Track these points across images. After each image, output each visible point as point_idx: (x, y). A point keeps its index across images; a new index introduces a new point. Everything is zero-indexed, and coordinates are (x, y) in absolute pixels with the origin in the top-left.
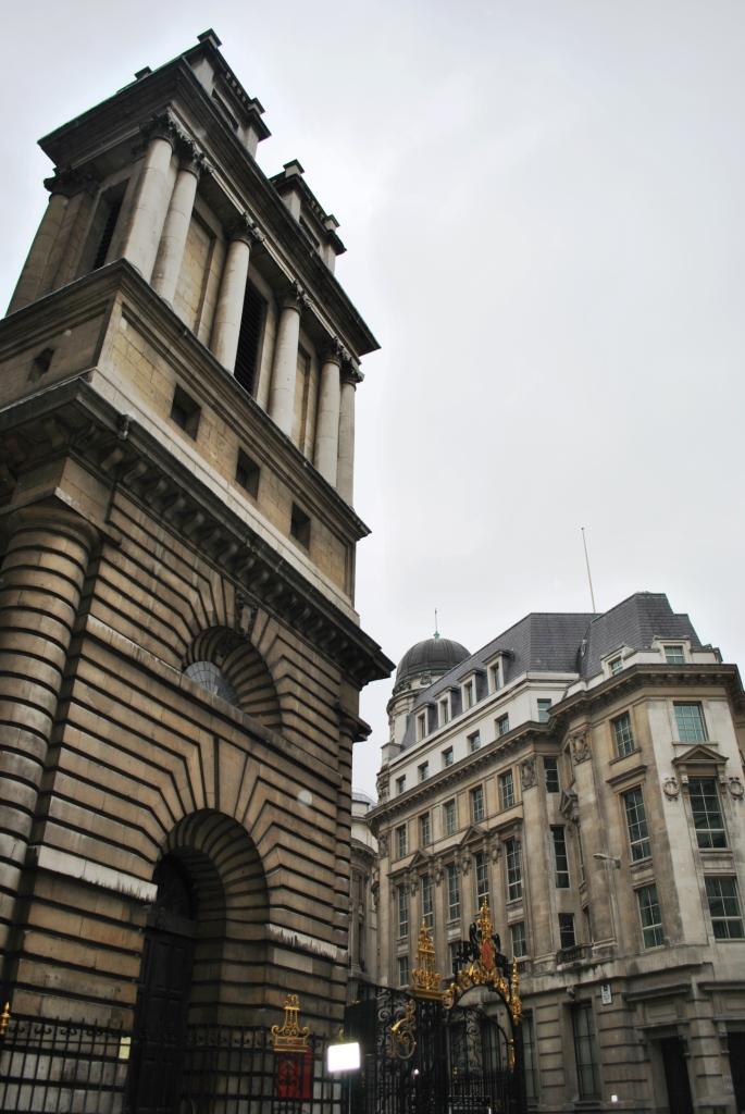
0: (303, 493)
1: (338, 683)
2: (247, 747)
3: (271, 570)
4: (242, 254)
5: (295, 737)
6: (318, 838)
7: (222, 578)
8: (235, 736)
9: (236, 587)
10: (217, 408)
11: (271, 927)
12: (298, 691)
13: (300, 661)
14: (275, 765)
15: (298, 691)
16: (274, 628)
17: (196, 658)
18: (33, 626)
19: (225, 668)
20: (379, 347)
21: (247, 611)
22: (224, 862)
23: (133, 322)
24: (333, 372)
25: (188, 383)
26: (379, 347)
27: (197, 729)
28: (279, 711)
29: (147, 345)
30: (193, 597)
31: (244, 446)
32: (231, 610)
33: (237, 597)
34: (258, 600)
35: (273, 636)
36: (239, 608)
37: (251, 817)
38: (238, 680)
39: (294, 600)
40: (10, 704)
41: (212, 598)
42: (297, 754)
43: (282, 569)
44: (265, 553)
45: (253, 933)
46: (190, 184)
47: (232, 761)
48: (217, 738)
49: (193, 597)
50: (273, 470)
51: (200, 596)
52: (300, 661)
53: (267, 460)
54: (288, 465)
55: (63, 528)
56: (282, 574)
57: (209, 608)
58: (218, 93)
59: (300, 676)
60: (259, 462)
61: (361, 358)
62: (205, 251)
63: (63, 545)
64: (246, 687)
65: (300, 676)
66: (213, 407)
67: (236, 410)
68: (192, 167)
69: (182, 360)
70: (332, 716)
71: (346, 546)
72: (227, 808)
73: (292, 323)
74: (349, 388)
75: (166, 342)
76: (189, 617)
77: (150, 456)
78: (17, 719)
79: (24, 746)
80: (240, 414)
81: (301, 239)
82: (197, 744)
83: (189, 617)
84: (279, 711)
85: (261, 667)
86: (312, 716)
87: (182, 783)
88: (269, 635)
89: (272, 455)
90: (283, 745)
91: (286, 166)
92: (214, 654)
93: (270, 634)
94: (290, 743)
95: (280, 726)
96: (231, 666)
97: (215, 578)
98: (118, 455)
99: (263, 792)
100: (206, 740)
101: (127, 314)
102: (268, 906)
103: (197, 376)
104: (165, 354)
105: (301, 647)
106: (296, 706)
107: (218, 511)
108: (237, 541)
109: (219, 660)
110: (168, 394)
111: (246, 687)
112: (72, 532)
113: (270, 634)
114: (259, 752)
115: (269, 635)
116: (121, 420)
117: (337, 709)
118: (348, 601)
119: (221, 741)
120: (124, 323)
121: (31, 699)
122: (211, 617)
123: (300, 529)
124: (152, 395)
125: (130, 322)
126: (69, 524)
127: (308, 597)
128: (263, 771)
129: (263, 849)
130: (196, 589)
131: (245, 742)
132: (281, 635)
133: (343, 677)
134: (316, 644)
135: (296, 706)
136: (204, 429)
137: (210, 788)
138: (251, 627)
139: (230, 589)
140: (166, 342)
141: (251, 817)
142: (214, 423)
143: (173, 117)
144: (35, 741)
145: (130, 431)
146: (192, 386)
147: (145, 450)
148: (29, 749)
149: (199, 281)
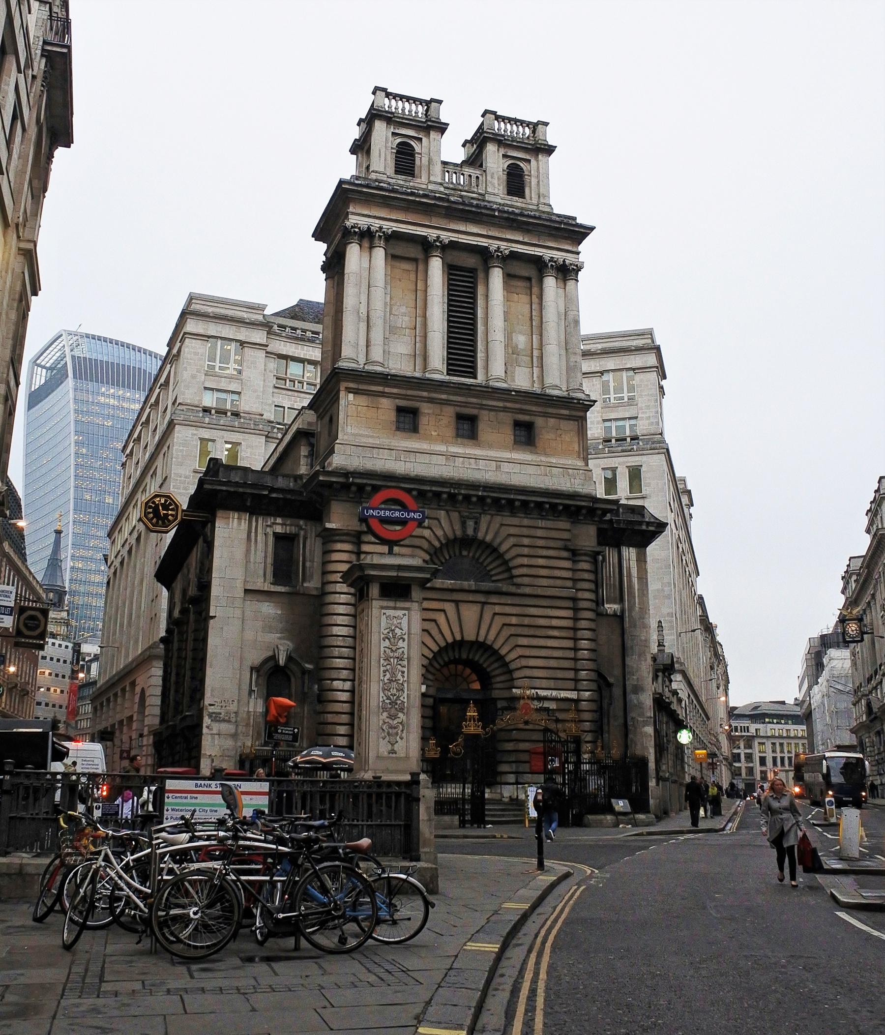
0: (521, 409)
1: (569, 530)
2: (483, 600)
3: (477, 496)
4: (436, 265)
5: (526, 580)
6: (556, 633)
7: (447, 511)
8: (471, 597)
9: (459, 512)
10: (431, 401)
11: (514, 690)
12: (526, 551)
13: (525, 531)
14: (509, 602)
15: (526, 551)
16: (498, 520)
17: (447, 558)
18: (333, 590)
19: (471, 555)
20: (592, 229)
21: (471, 524)
22: (485, 661)
23: (356, 392)
24: (550, 282)
25: (404, 399)
26: (592, 229)
27: (442, 603)
28: (509, 569)
29: (370, 398)
30: (427, 533)
31: (458, 409)
32: (457, 527)
33: (461, 517)
34: (480, 511)
35: (498, 525)
36: (464, 524)
37: (491, 637)
38: (481, 560)
39: (503, 502)
40: (330, 628)
41: (443, 525)
42: (527, 590)
43: (484, 491)
44: (466, 489)
45: (506, 694)
46: (379, 254)
47: (470, 613)
48: (457, 602)
49: (427, 533)
50: (490, 410)
51: (432, 530)
52: (525, 531)
53: (482, 407)
54: (499, 400)
55: (337, 538)
56: (485, 494)
57: (440, 533)
58: (397, 131)
59: (526, 541)
60: (474, 412)
61: (581, 248)
62: (412, 276)
63: (339, 546)
64: (489, 560)
65: (526, 541)
66: (428, 402)
67: (443, 393)
68: (376, 242)
69: (395, 391)
70: (565, 554)
71: (577, 420)
72: (470, 636)
73: (497, 276)
74: (570, 284)
75: (380, 389)
76: (426, 545)
77: (369, 482)
78: (334, 633)
79: (339, 644)
80: (449, 394)
81: (483, 211)
82: (444, 611)
83: (426, 545)
84: (509, 569)
85: (492, 549)
86: (541, 562)
87: (435, 632)
88: (490, 528)
89: (484, 402)
90: (513, 589)
91: (483, 116)
92: (460, 553)
93: (495, 526)
94: (518, 585)
95: (512, 577)
96: (476, 552)
97: (443, 513)
98: (354, 488)
99: (499, 621)
100: (449, 607)
101: (349, 390)
102: (513, 680)
103: (410, 392)
104: (383, 395)
105: (526, 522)
106: (525, 561)
107: (424, 484)
108: (445, 492)
109: (465, 553)
110: (392, 416)
111: (489, 560)
112: (344, 538)
113: (495, 526)
114: (494, 599)
115: (490, 528)
116: (347, 474)
117: (566, 549)
118: (580, 463)
119: (461, 604)
120: (351, 396)
121: (339, 623)
122: (442, 539)
123: (526, 434)
124: (380, 427)
125: (354, 393)
126: (338, 535)
127: (512, 497)
128: (498, 609)
129: (503, 652)
130: (429, 528)
131: (481, 598)
132: (504, 522)
133: (572, 523)
134: (539, 514)
135: (525, 561)
136: (423, 421)
137: (456, 630)
138: (476, 530)
139: (455, 515)
140: (380, 389)
141: (491, 637)
142: (430, 411)
143: (352, 220)
144: (344, 640)
145: (353, 478)
146: (408, 400)
147: (365, 481)
148: (342, 644)
149: (412, 304)
